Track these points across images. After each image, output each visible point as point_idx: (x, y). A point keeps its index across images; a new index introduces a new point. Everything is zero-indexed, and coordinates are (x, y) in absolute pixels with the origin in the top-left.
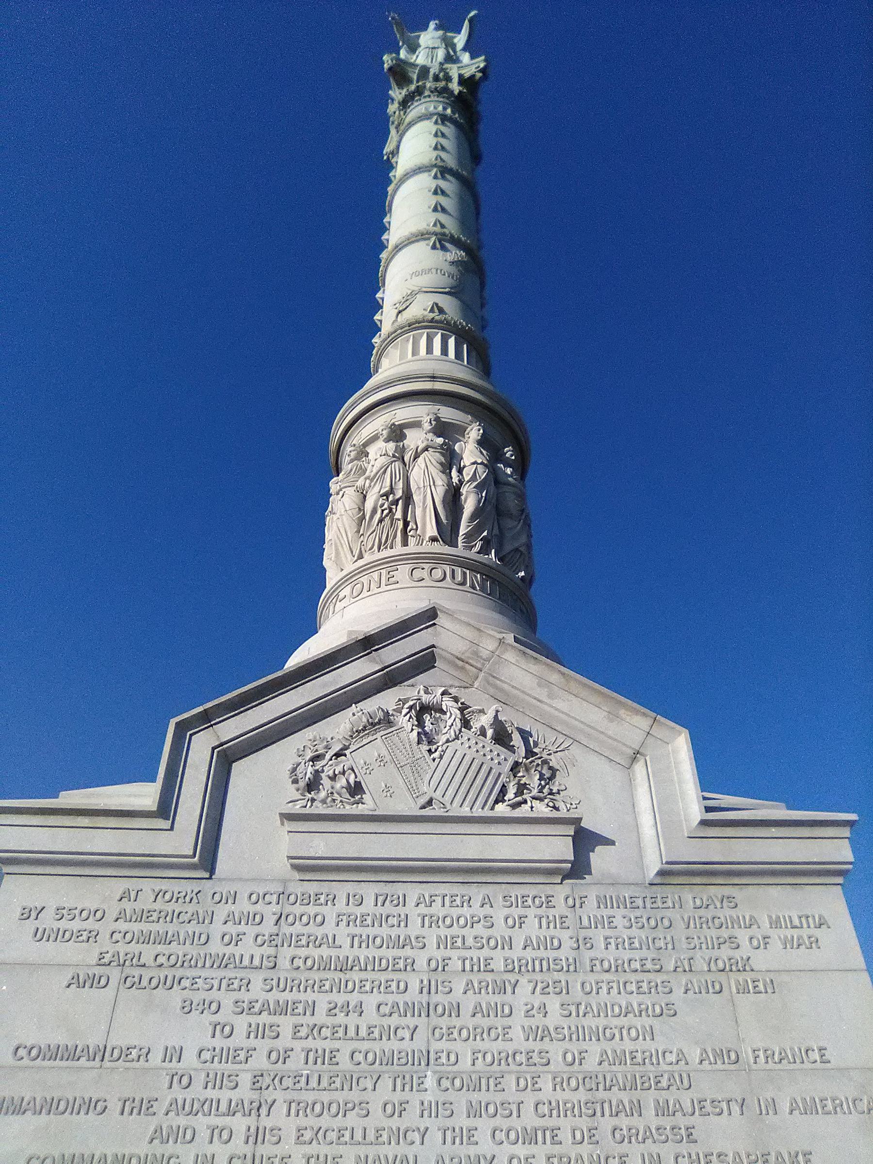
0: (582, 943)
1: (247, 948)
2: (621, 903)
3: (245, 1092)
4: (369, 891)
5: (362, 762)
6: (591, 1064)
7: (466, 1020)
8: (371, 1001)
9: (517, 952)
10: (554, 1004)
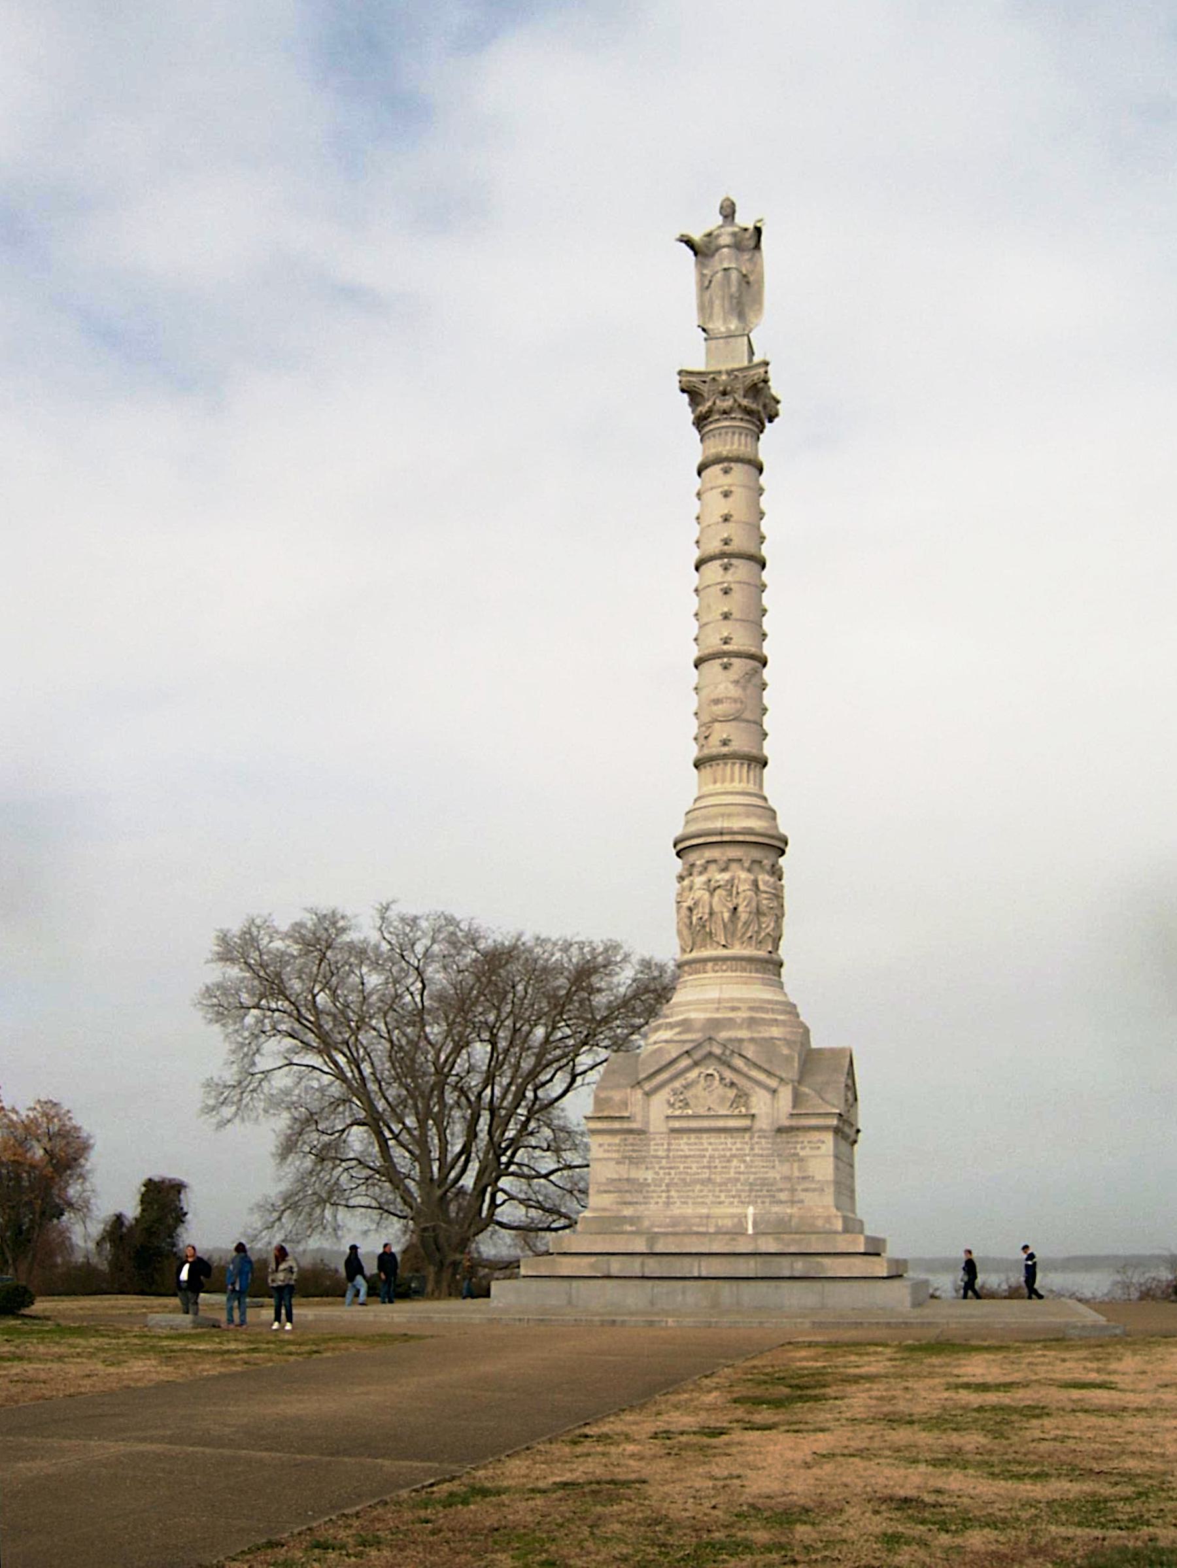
0: (752, 1149)
1: (660, 1153)
2: (765, 1137)
3: (664, 1188)
4: (693, 1136)
5: (731, 686)
6: (751, 1180)
9: (734, 1152)
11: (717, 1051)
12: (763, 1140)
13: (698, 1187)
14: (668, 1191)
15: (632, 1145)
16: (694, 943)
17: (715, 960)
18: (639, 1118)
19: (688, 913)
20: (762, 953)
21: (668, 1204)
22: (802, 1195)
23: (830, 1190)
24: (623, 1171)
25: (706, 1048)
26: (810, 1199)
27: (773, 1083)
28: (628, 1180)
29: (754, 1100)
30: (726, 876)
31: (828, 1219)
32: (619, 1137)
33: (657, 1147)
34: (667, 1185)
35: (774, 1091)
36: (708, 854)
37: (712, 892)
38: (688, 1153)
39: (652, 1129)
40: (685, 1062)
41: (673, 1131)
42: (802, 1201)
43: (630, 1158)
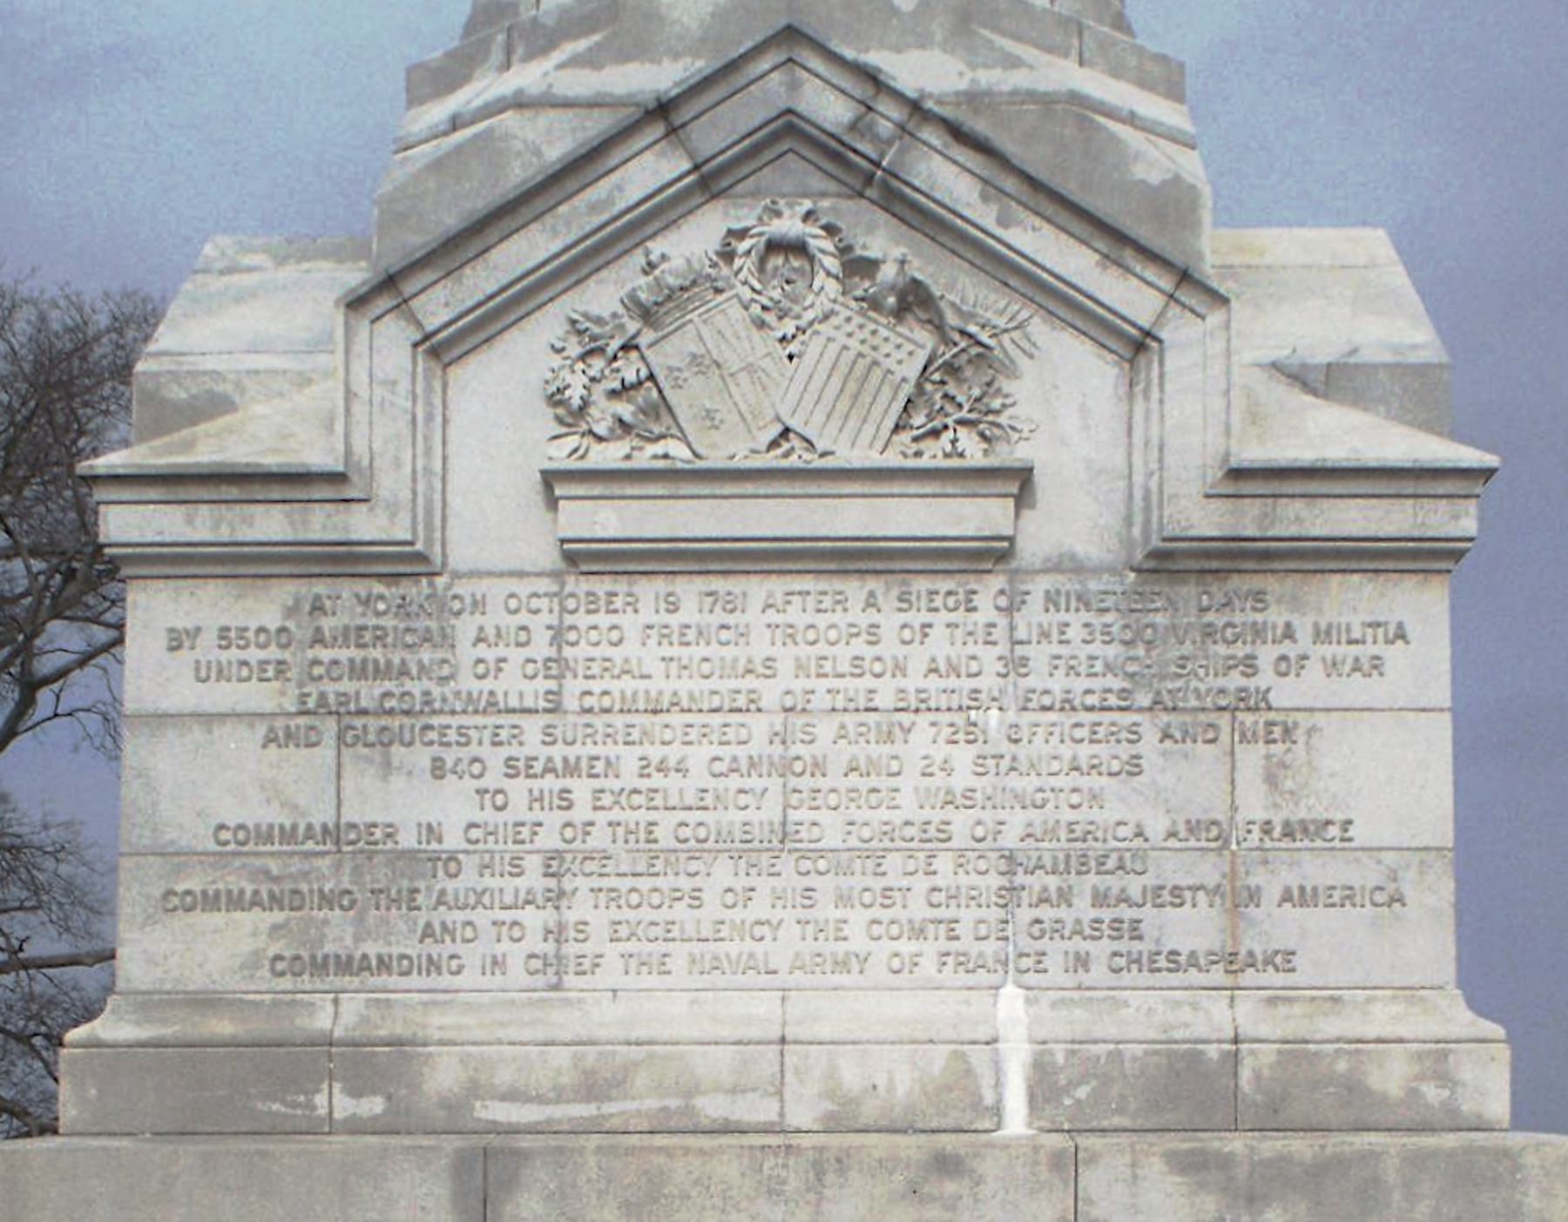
0: (1016, 665)
1: (514, 686)
2: (1084, 601)
3: (533, 878)
4: (689, 590)
6: (1010, 839)
7: (834, 779)
8: (698, 756)
9: (914, 681)
10: (964, 756)
11: (829, 107)
12: (1076, 620)
13: (723, 873)
14: (557, 898)
15: (354, 635)
18: (391, 483)
21: (553, 969)
22: (1274, 925)
23: (1433, 895)
24: (305, 786)
25: (767, 92)
26: (1327, 943)
27: (1132, 296)
28: (333, 834)
29: (1024, 395)
31: (1437, 1059)
32: (286, 591)
33: (496, 644)
34: (554, 864)
35: (1137, 346)
38: (661, 686)
39: (461, 554)
40: (649, 170)
41: (580, 557)
42: (1283, 960)
43: (344, 712)
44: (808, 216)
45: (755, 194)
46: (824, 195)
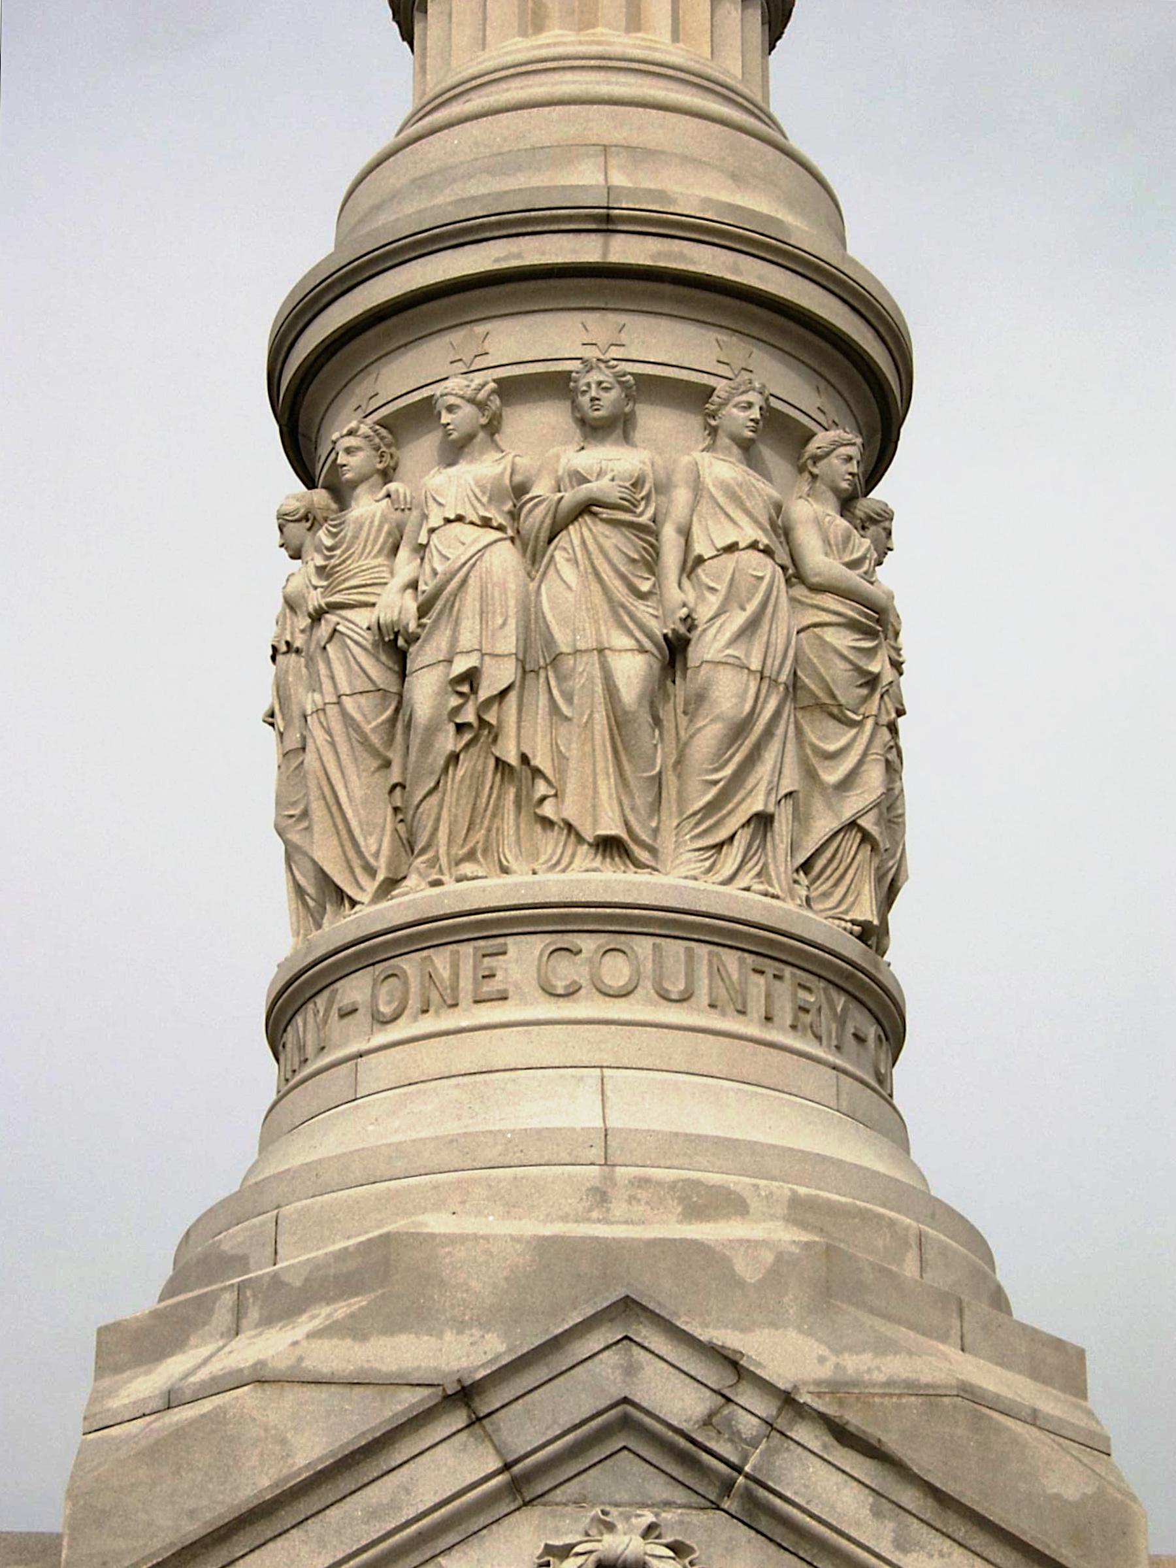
11: (677, 1399)
16: (408, 845)
17: (561, 921)
19: (378, 671)
20: (823, 923)
30: (610, 464)
36: (521, 340)
37: (536, 551)
44: (650, 1531)
45: (579, 1502)
46: (668, 1504)
